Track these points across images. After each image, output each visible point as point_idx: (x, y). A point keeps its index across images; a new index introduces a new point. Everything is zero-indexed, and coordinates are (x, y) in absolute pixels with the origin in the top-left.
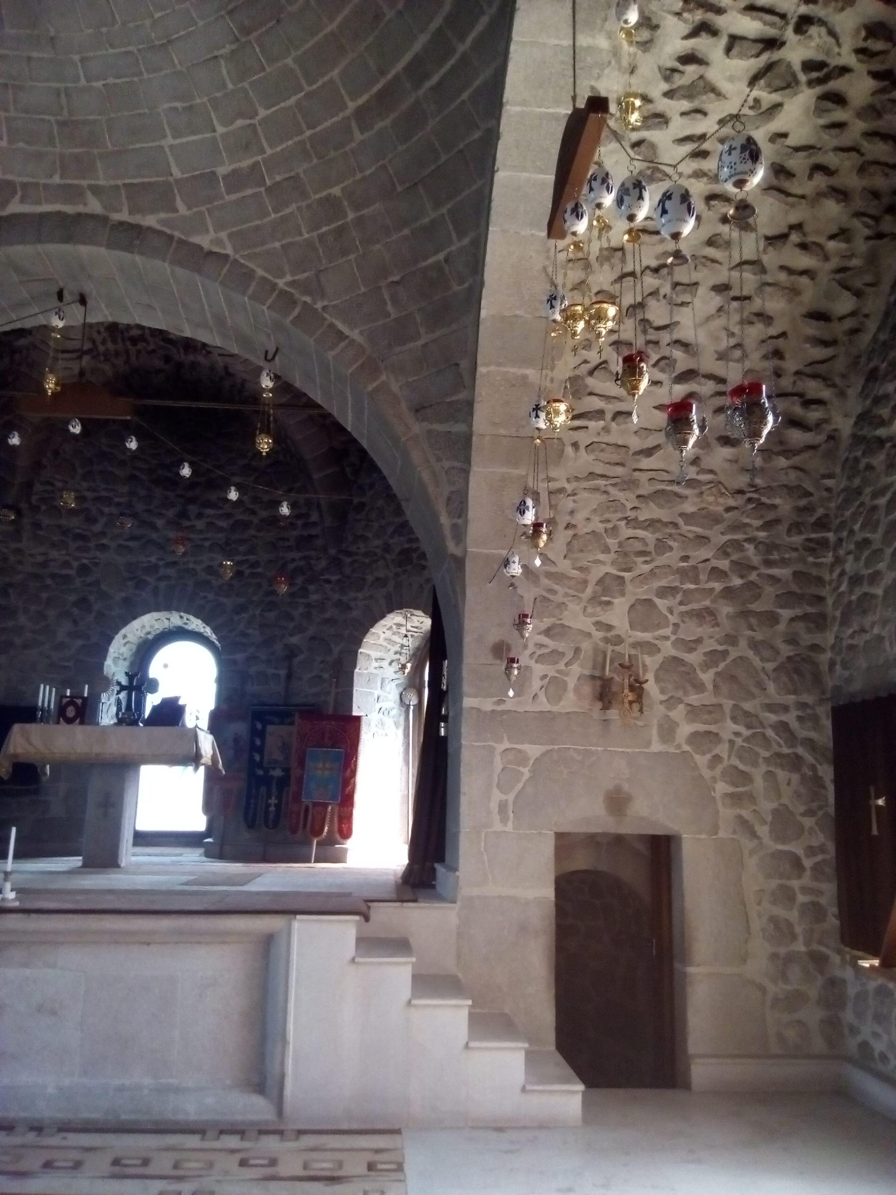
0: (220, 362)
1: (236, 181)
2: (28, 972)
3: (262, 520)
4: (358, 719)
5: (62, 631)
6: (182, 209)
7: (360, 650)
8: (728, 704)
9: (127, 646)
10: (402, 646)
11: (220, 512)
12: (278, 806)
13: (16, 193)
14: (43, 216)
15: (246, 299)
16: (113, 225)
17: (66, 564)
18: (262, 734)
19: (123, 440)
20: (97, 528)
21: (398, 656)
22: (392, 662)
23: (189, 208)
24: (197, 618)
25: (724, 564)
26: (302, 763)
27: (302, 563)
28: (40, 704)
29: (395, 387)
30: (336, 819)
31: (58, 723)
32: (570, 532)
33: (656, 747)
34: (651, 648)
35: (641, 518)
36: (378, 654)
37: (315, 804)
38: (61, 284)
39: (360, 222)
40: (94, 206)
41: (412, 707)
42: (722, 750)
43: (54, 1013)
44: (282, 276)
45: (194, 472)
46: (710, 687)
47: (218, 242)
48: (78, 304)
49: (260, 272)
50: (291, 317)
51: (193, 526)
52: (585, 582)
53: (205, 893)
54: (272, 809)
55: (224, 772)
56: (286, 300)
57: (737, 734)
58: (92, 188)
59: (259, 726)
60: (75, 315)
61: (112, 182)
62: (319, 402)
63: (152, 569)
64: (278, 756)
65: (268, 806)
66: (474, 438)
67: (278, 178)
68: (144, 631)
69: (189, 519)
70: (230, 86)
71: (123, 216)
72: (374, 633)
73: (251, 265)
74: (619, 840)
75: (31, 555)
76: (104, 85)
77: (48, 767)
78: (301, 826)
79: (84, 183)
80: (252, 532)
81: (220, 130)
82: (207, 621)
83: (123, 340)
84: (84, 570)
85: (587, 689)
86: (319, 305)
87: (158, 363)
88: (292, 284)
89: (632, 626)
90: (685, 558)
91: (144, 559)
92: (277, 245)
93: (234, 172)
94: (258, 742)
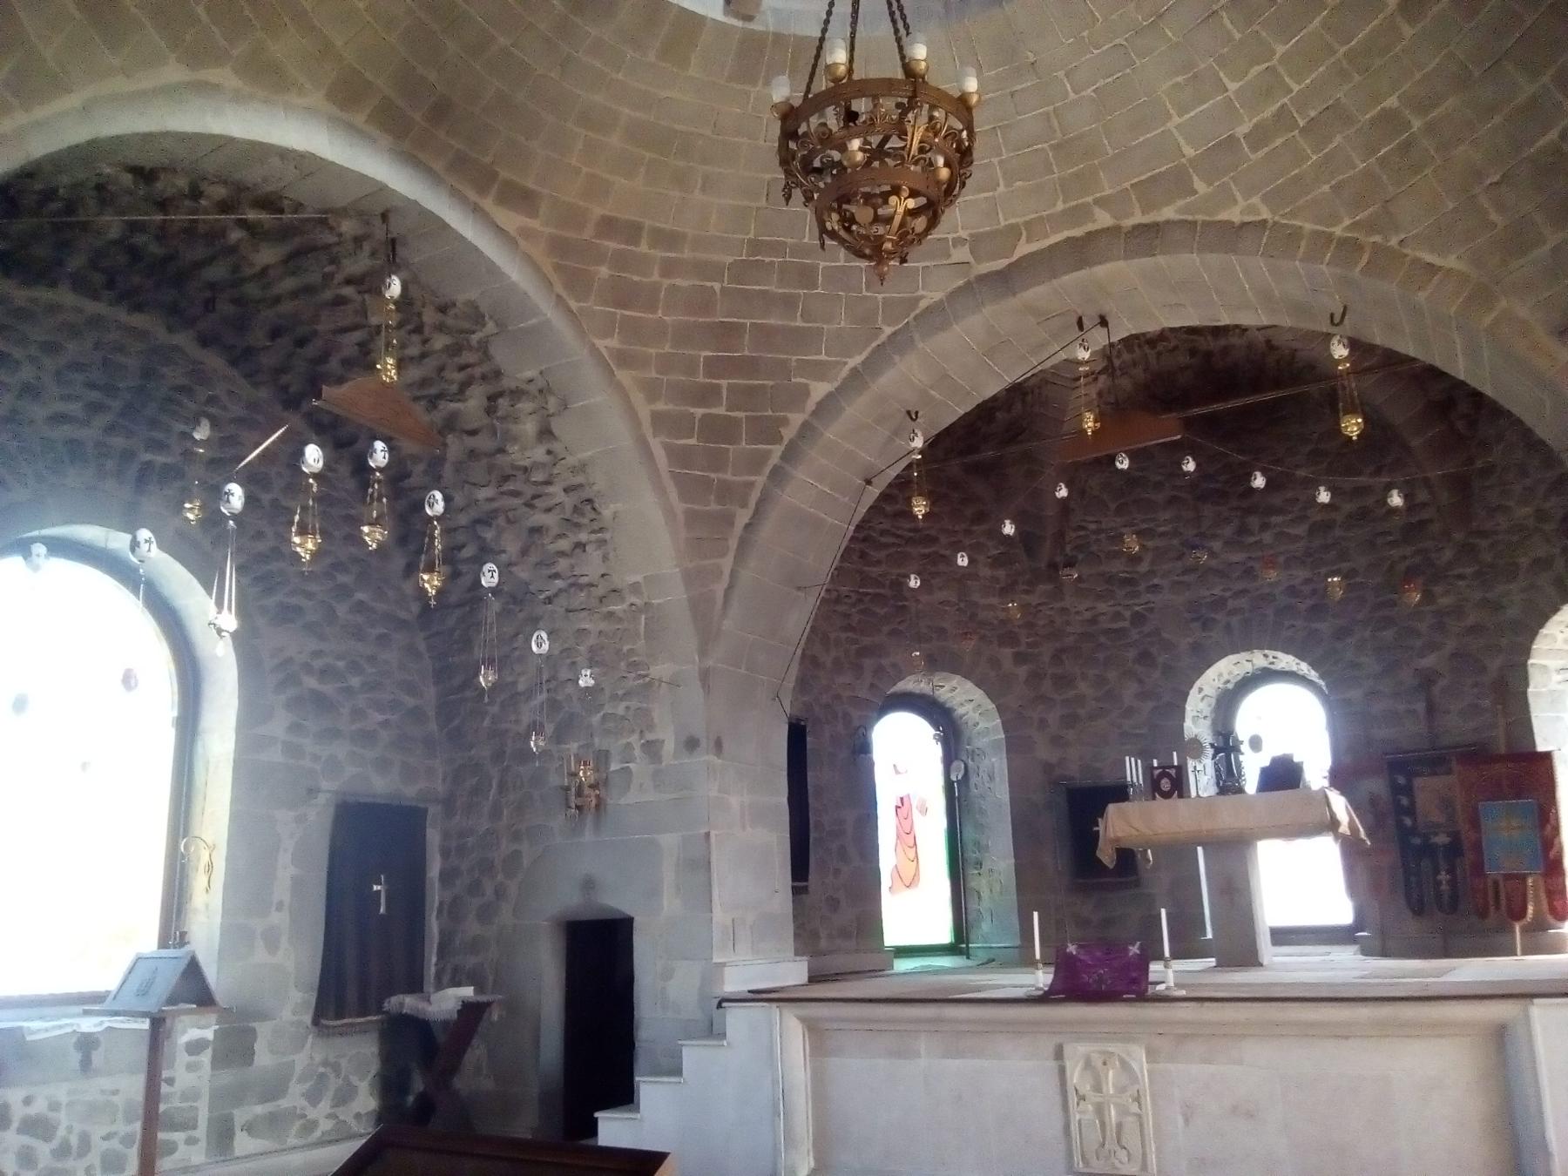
0: (1260, 337)
1: (1259, 137)
2: (1212, 1068)
3: (1350, 516)
5: (1130, 691)
6: (1201, 186)
7: (1530, 662)
9: (1205, 700)
11: (1290, 517)
12: (1453, 883)
13: (1021, 234)
14: (1051, 247)
15: (1297, 262)
16: (1129, 232)
17: (1117, 616)
18: (1408, 790)
19: (1179, 464)
20: (1144, 567)
23: (1210, 184)
24: (1287, 653)
26: (1475, 823)
27: (1417, 559)
28: (1129, 779)
29: (1522, 312)
30: (1543, 896)
31: (1154, 798)
37: (1508, 877)
38: (1080, 312)
39: (1430, 128)
40: (1103, 219)
43: (1250, 1115)
44: (1340, 221)
47: (1251, 209)
48: (1099, 326)
49: (1308, 226)
50: (1358, 269)
51: (1260, 541)
53: (1397, 984)
54: (1444, 887)
55: (1369, 843)
56: (1349, 248)
58: (1097, 202)
59: (1401, 780)
60: (1099, 338)
61: (1119, 188)
62: (1412, 353)
63: (1219, 603)
64: (1437, 817)
65: (1439, 883)
67: (1313, 114)
68: (1223, 680)
69: (1252, 534)
70: (1238, 36)
71: (1138, 218)
72: (1546, 635)
73: (1297, 223)
75: (1077, 613)
76: (1094, 91)
77: (1149, 851)
78: (1492, 909)
79: (1090, 199)
80: (1338, 532)
81: (1233, 86)
82: (1301, 656)
83: (1140, 346)
84: (1139, 619)
86: (1394, 242)
87: (1183, 359)
88: (1348, 228)
91: (1207, 593)
92: (1326, 188)
93: (1256, 126)
94: (1405, 801)
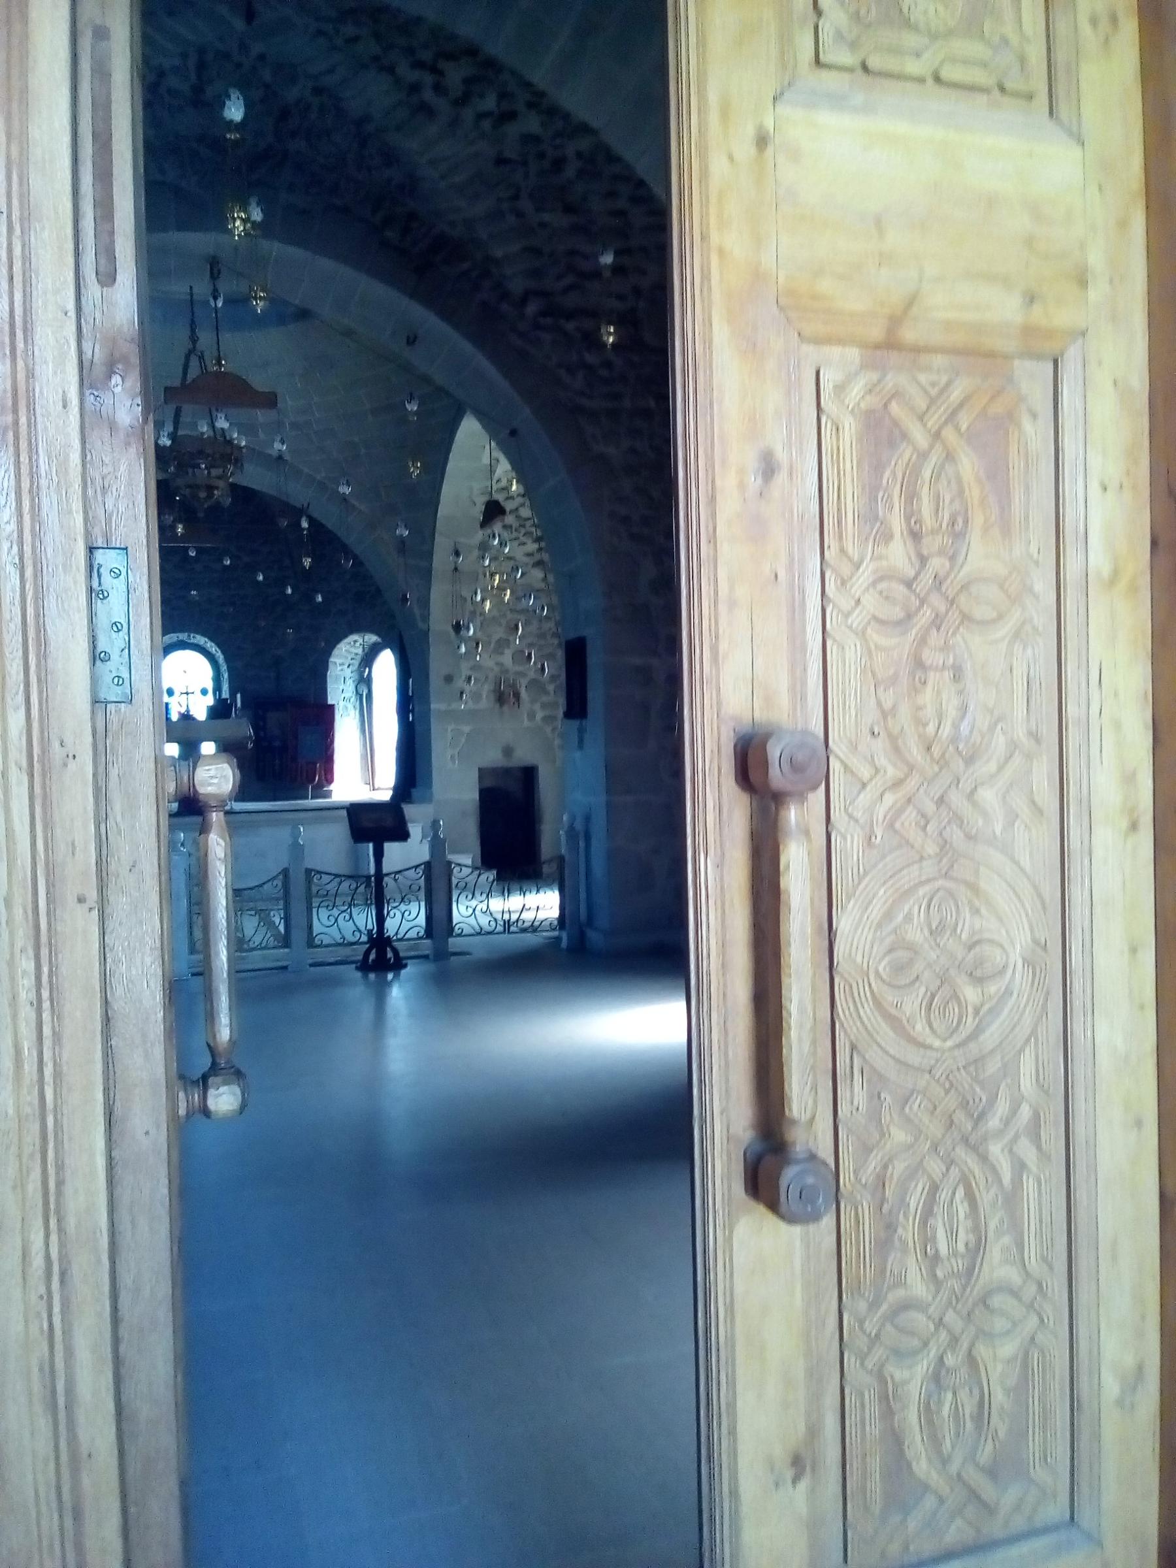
4: (332, 706)
10: (357, 654)
21: (351, 662)
22: (349, 665)
30: (323, 772)
32: (482, 618)
45: (264, 578)
46: (552, 692)
52: (490, 643)
59: (260, 712)
74: (506, 772)
81: (290, 403)
85: (492, 697)
94: (261, 724)
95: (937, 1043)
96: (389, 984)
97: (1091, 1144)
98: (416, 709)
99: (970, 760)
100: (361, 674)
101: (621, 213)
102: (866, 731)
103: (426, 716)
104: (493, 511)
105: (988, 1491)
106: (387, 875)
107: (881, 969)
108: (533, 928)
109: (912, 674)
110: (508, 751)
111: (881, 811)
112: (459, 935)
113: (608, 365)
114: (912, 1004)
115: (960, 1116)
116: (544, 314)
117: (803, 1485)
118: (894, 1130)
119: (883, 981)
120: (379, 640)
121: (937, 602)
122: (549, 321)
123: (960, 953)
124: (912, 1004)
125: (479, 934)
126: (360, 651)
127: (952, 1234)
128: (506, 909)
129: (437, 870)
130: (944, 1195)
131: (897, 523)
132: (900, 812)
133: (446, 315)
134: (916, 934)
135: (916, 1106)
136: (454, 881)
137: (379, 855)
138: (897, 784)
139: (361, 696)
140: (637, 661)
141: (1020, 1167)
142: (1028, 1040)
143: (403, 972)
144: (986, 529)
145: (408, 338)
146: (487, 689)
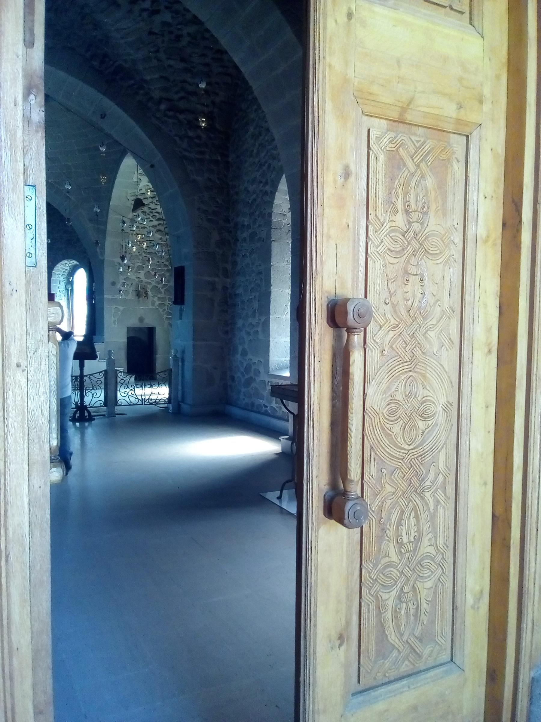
7: (53, 272)
8: (167, 297)
10: (66, 270)
25: (167, 263)
32: (130, 255)
33: (151, 307)
34: (150, 283)
35: (148, 252)
36: (58, 273)
41: (70, 290)
42: (166, 308)
52: (134, 267)
57: (169, 304)
66: (107, 232)
74: (140, 329)
85: (134, 293)
89: (145, 279)
90: (158, 262)
95: (406, 447)
96: (87, 428)
97: (467, 493)
98: (97, 298)
99: (425, 318)
100: (68, 279)
101: (207, 65)
102: (382, 301)
103: (102, 301)
104: (138, 204)
105: (419, 648)
106: (86, 376)
107: (384, 412)
108: (156, 403)
109: (403, 277)
110: (141, 320)
111: (387, 339)
112: (120, 405)
113: (199, 137)
114: (397, 429)
115: (415, 479)
116: (170, 110)
117: (343, 648)
118: (387, 486)
119: (386, 418)
120: (78, 263)
121: (414, 243)
122: (171, 113)
123: (417, 406)
124: (397, 429)
125: (130, 405)
126: (68, 268)
127: (409, 534)
128: (143, 394)
129: (110, 375)
130: (406, 515)
131: (400, 206)
132: (396, 340)
133: (121, 105)
134: (399, 397)
135: (397, 475)
136: (119, 380)
137: (82, 366)
138: (395, 327)
139: (68, 290)
140: (209, 279)
141: (437, 503)
142: (443, 447)
143: (93, 422)
144: (437, 211)
145: (101, 115)
146: (131, 290)
